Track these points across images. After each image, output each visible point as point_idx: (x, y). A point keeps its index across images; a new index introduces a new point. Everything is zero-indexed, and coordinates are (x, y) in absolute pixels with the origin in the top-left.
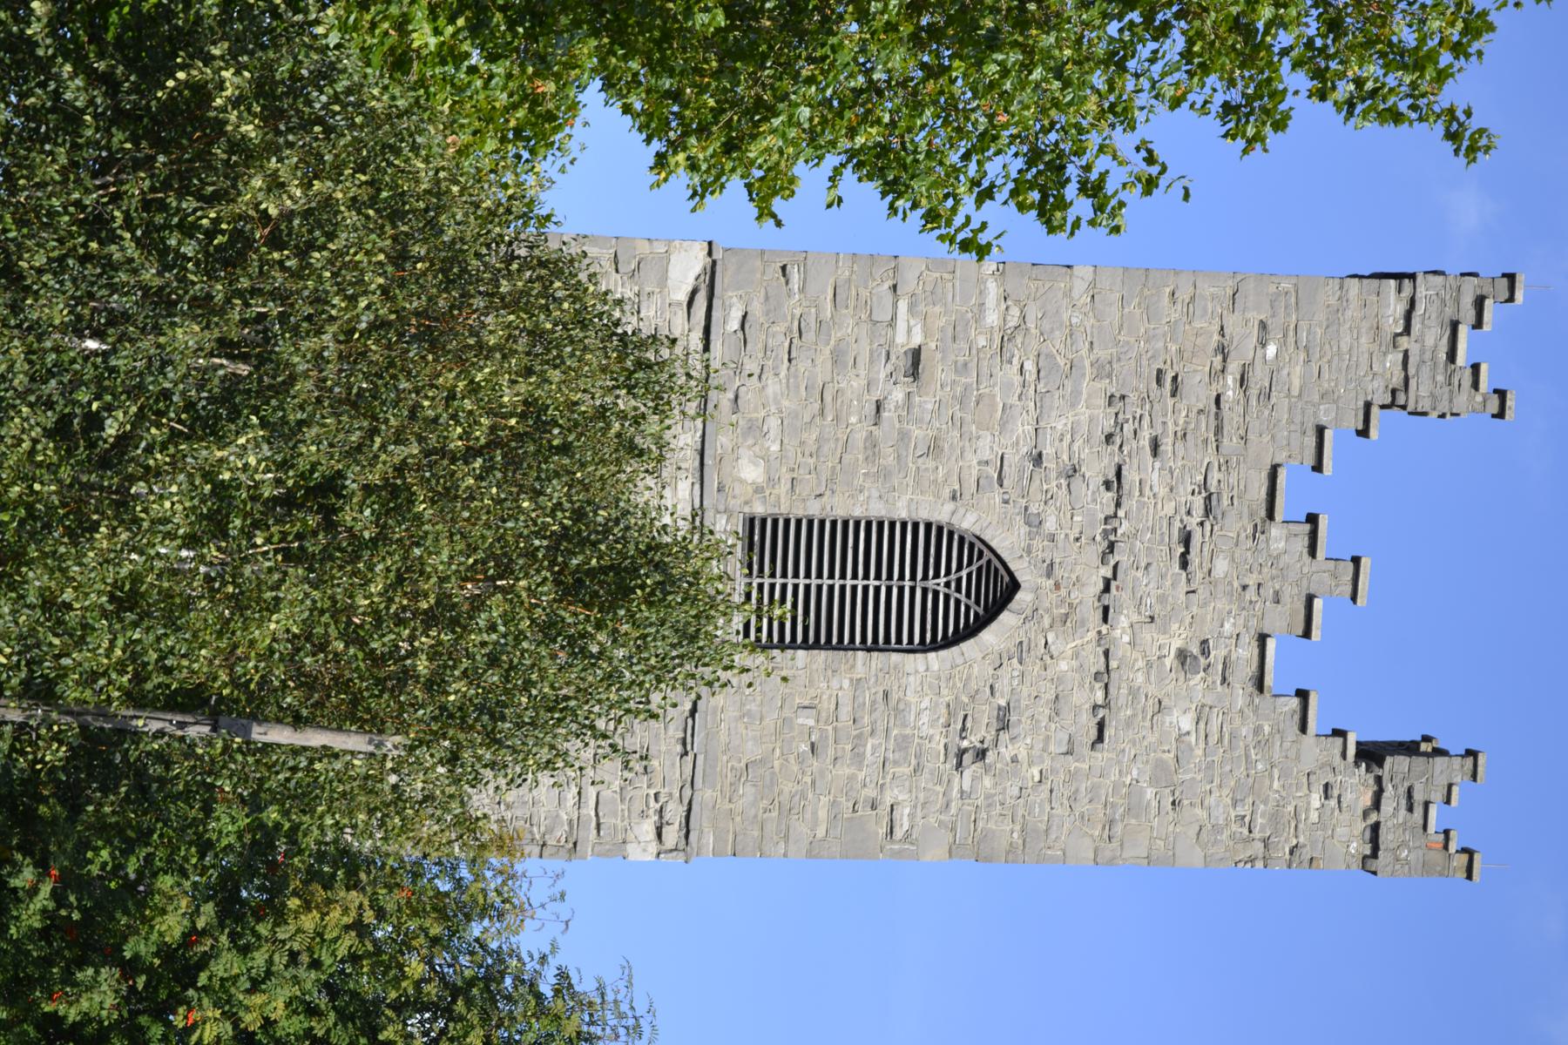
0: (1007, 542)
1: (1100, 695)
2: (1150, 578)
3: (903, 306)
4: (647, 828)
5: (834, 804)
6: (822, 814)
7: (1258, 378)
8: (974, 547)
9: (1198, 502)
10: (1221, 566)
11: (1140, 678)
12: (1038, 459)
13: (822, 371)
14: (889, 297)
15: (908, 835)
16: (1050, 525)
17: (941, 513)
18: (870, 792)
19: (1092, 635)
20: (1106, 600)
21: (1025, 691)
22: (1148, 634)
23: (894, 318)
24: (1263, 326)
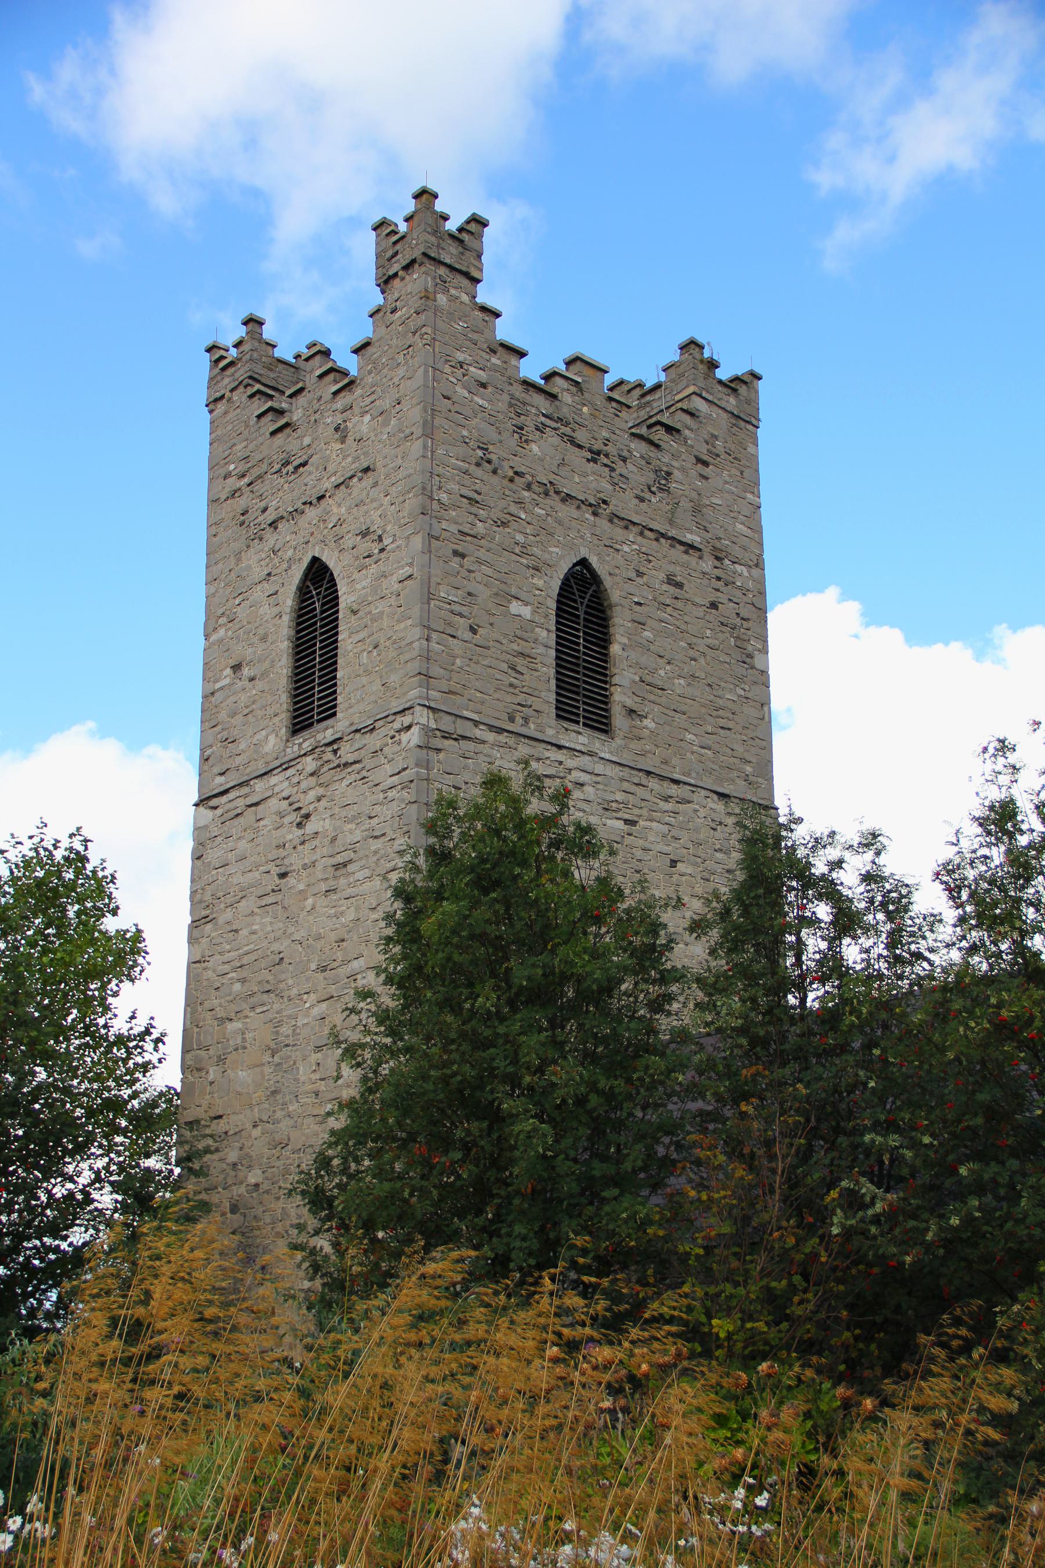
0: (297, 573)
1: (355, 480)
2: (312, 481)
3: (218, 686)
4: (405, 737)
5: (399, 621)
6: (402, 625)
7: (242, 467)
8: (303, 592)
9: (284, 471)
10: (307, 441)
11: (350, 459)
12: (269, 574)
13: (239, 719)
14: (217, 695)
15: (411, 565)
16: (290, 553)
17: (286, 618)
18: (393, 600)
19: (330, 501)
20: (315, 502)
21: (353, 527)
22: (331, 468)
23: (221, 688)
24: (225, 478)
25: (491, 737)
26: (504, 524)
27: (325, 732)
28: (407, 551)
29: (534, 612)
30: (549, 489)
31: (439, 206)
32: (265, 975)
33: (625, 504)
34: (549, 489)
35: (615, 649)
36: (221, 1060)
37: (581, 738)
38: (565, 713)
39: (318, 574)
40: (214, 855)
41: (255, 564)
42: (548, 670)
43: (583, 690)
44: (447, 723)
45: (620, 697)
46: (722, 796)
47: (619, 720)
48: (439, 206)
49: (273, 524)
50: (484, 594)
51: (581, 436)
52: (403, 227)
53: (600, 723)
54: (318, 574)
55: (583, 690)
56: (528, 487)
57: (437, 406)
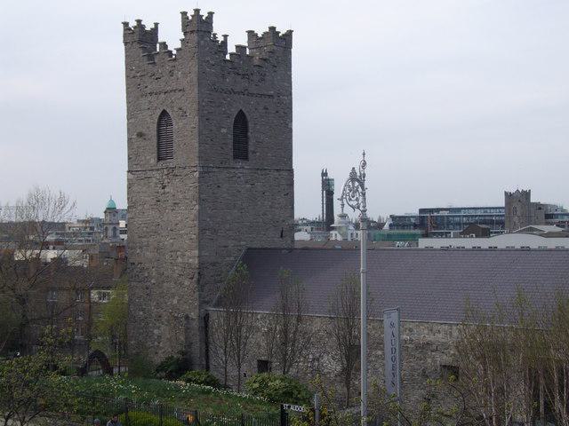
0: (159, 112)
25: (216, 170)
26: (219, 106)
27: (171, 163)
28: (192, 121)
29: (227, 130)
30: (232, 92)
31: (201, 14)
32: (154, 228)
33: (253, 89)
34: (232, 92)
35: (249, 134)
36: (140, 248)
37: (240, 164)
38: (236, 157)
39: (164, 113)
40: (134, 188)
41: (144, 102)
42: (231, 147)
43: (241, 152)
44: (206, 170)
45: (251, 148)
46: (277, 170)
47: (250, 155)
48: (201, 14)
49: (151, 94)
50: (214, 128)
51: (240, 72)
52: (190, 18)
53: (246, 158)
54: (164, 113)
55: (241, 152)
56: (225, 93)
57: (202, 75)
